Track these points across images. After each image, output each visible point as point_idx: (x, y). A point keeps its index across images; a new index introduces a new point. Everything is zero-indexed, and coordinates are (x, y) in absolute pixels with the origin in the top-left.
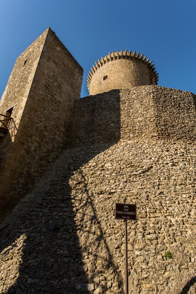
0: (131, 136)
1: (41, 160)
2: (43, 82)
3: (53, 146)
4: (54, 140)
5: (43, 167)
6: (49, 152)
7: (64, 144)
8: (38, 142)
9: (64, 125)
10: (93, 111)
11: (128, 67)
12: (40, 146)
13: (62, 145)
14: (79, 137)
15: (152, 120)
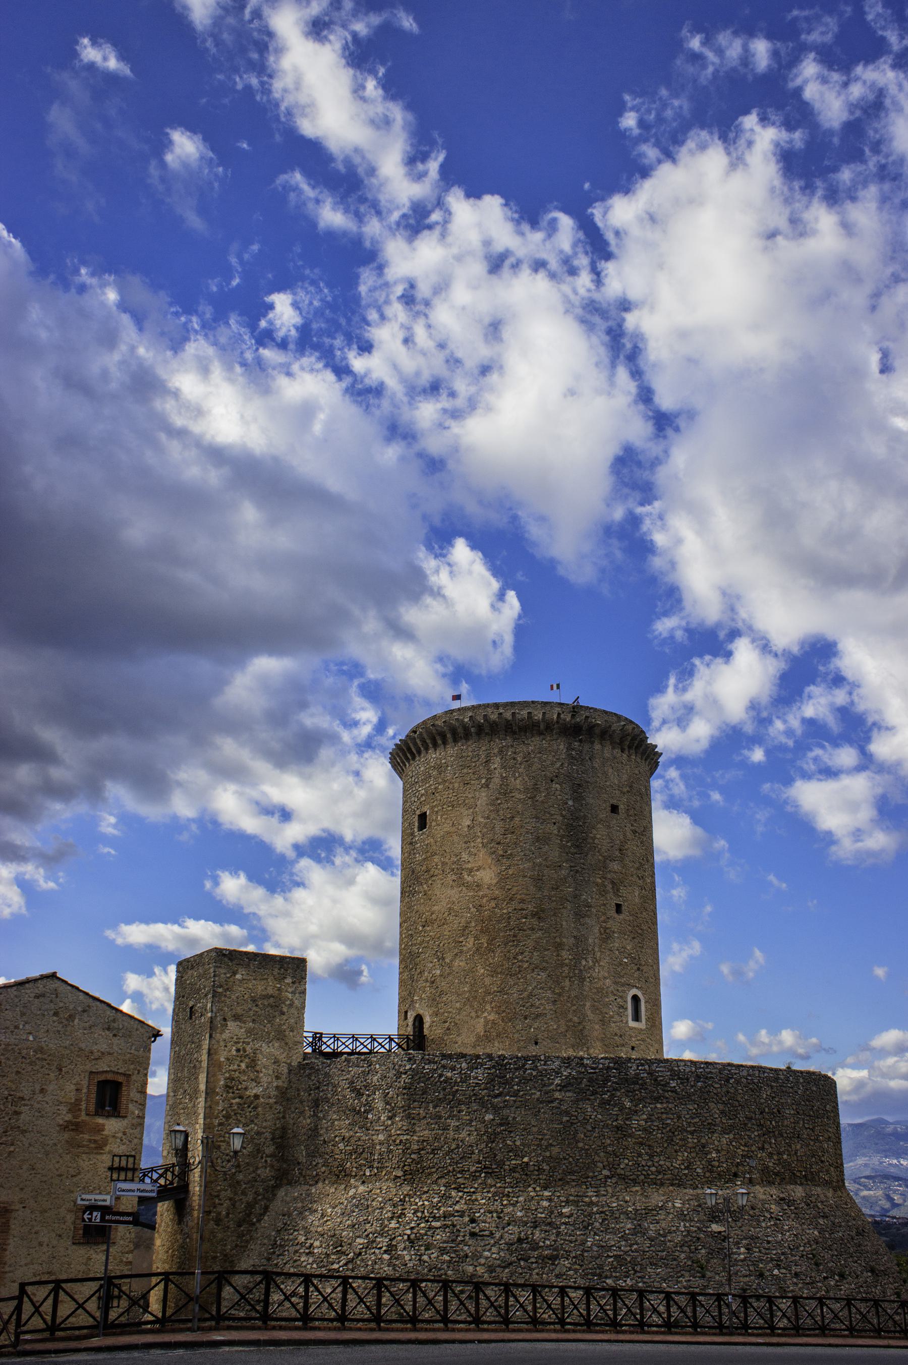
0: (368, 1174)
1: (240, 1226)
2: (222, 1083)
3: (255, 1193)
4: (256, 1181)
5: (244, 1236)
6: (250, 1206)
7: (277, 1179)
8: (230, 1199)
9: (272, 1139)
10: (316, 1103)
11: (483, 781)
12: (234, 1205)
13: (273, 1182)
14: (299, 1163)
15: (398, 1141)
